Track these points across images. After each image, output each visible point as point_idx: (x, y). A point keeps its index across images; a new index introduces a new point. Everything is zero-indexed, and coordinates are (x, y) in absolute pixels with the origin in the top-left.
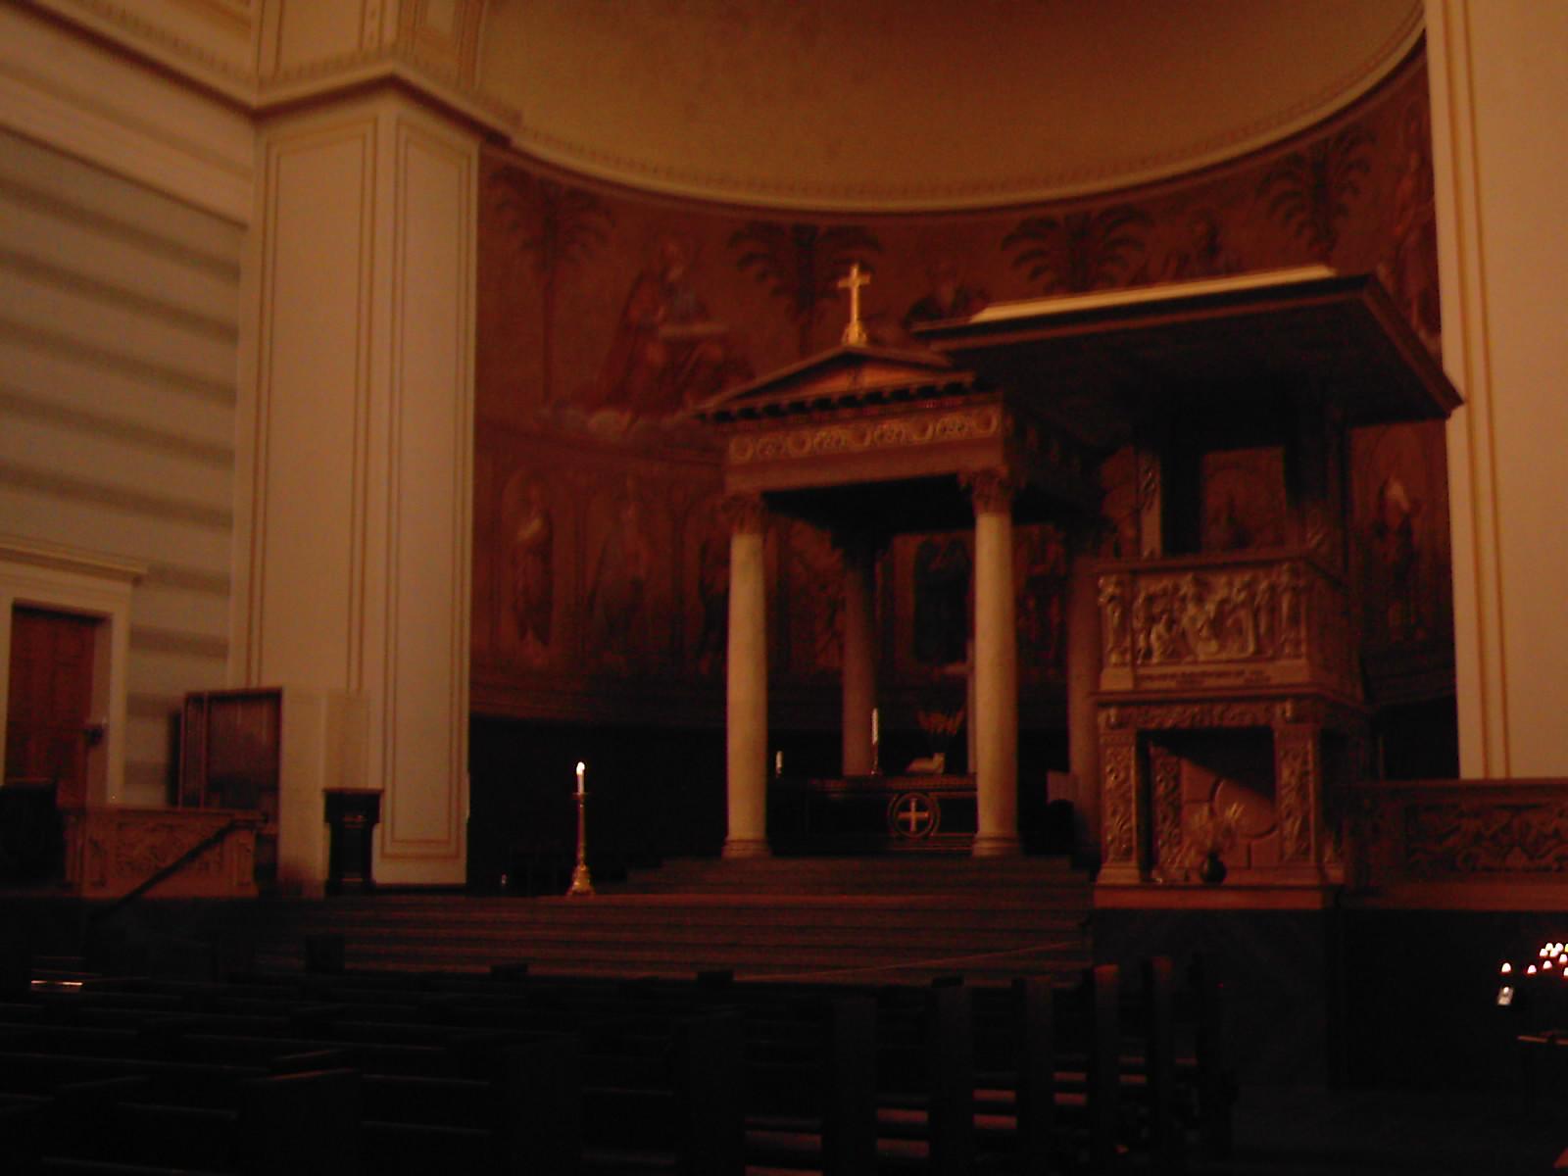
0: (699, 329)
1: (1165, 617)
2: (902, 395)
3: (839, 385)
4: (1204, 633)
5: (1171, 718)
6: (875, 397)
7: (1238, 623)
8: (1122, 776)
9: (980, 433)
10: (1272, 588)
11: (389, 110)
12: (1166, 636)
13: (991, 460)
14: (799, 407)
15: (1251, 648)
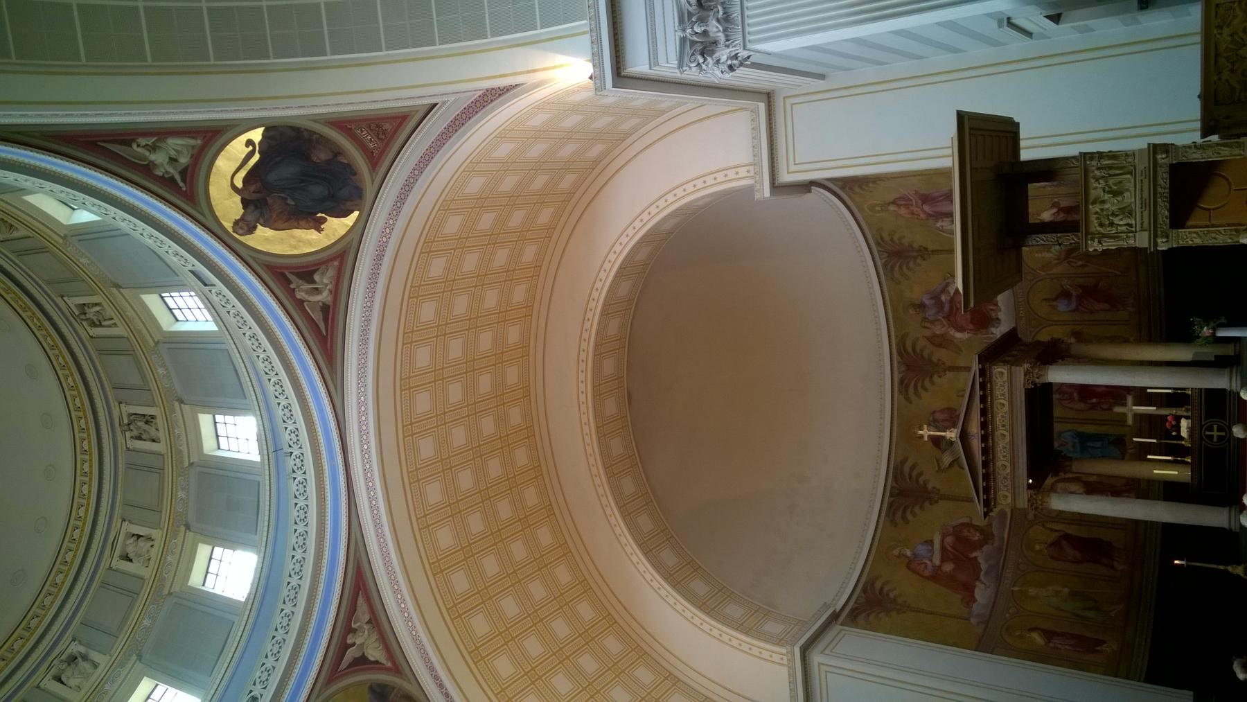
0: (937, 545)
1: (1111, 218)
2: (984, 412)
3: (976, 445)
4: (1120, 199)
5: (1164, 213)
6: (984, 425)
7: (1115, 184)
8: (1195, 235)
9: (1005, 377)
10: (1098, 169)
11: (816, 658)
12: (1121, 217)
13: (1020, 371)
14: (985, 464)
15: (1128, 176)
